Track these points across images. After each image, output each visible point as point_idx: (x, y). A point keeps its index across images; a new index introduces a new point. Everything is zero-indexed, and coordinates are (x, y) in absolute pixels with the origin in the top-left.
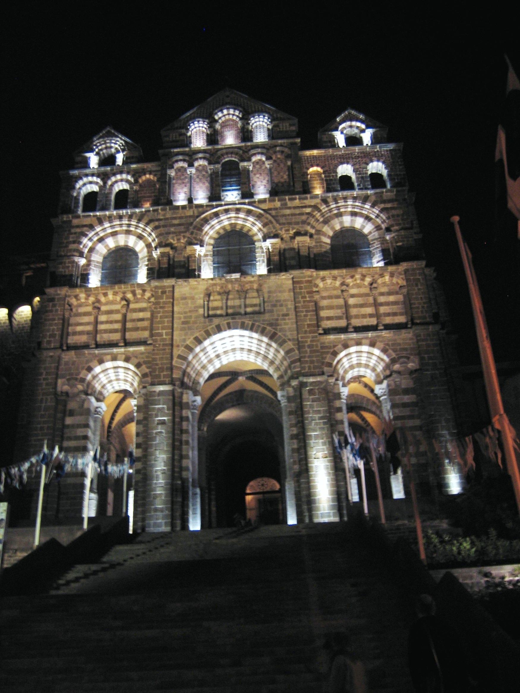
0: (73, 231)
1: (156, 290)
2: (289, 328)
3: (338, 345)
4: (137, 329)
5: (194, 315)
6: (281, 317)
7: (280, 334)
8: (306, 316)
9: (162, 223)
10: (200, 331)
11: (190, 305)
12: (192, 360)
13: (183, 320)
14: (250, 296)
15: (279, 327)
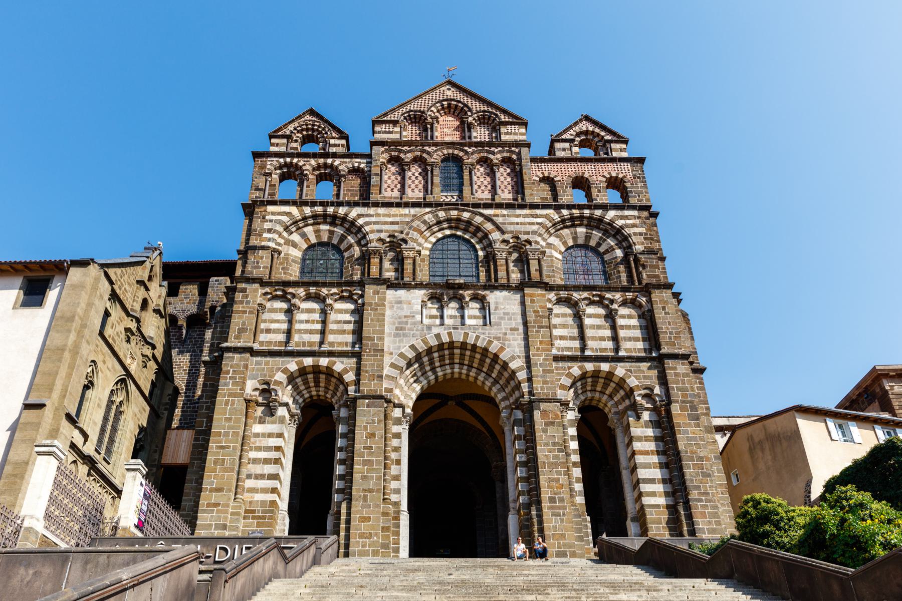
5: (410, 320)
6: (509, 332)
7: (507, 349)
8: (538, 332)
9: (373, 219)
10: (417, 339)
11: (405, 309)
13: (397, 325)
15: (506, 342)
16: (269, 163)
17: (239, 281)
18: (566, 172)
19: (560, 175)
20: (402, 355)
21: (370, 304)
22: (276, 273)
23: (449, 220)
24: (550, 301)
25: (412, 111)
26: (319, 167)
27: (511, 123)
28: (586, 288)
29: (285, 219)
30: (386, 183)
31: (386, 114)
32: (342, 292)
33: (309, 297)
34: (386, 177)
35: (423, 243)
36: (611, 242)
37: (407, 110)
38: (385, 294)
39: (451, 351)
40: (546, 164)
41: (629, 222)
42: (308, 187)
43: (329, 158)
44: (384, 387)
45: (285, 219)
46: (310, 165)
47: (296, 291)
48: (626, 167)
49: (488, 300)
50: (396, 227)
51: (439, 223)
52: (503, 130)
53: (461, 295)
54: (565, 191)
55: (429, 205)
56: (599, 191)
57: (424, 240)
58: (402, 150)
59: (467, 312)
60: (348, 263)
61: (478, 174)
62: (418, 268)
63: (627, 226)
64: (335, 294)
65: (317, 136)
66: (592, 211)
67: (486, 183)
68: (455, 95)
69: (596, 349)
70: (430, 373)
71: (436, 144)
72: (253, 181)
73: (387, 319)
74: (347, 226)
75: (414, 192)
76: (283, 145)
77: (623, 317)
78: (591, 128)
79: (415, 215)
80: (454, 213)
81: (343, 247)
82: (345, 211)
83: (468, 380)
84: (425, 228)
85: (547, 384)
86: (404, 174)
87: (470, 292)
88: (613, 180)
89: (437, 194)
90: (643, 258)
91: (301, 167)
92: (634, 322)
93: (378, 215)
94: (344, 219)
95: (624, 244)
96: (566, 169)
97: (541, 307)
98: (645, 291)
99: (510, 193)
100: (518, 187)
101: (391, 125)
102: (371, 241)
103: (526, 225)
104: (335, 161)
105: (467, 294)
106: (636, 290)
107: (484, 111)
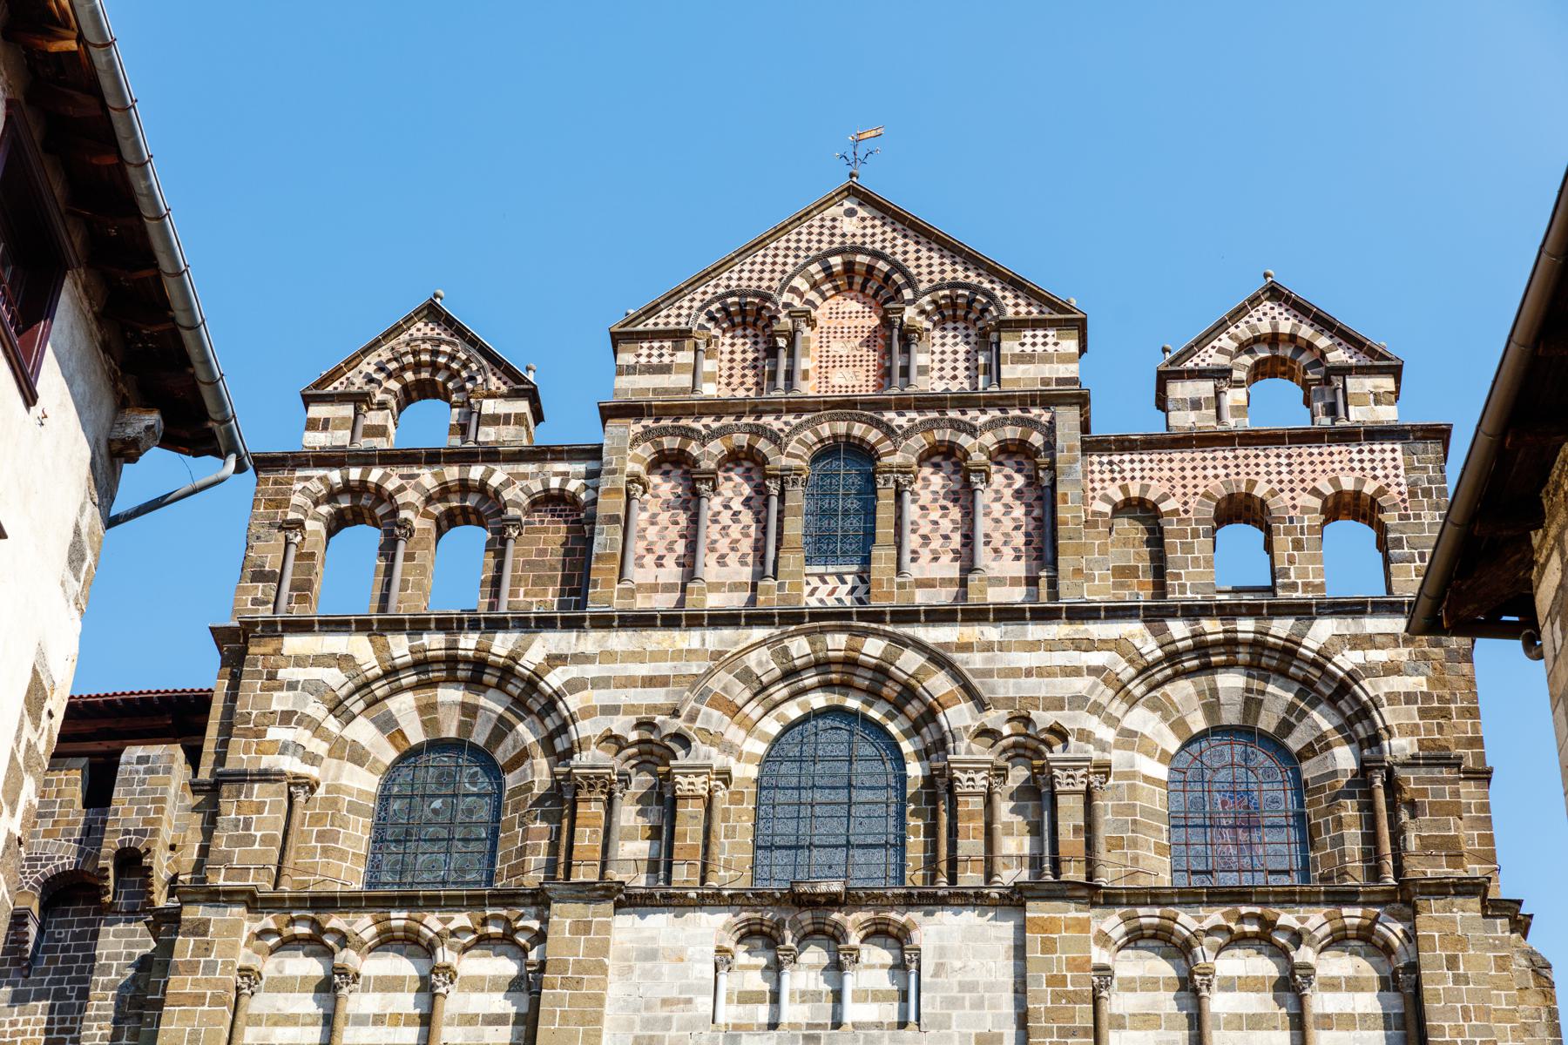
5: (678, 1015)
9: (591, 671)
13: (638, 1031)
16: (298, 486)
17: (189, 898)
18: (1199, 481)
19: (1179, 491)
21: (562, 966)
22: (298, 853)
23: (821, 665)
24: (1104, 939)
25: (732, 294)
26: (445, 491)
27: (1035, 324)
28: (1217, 896)
29: (334, 677)
30: (643, 538)
31: (652, 310)
32: (484, 922)
33: (387, 941)
34: (645, 516)
35: (738, 741)
36: (1323, 720)
37: (721, 290)
38: (608, 931)
40: (1136, 457)
42: (409, 557)
43: (476, 462)
45: (334, 677)
46: (418, 487)
47: (350, 924)
48: (1388, 455)
49: (916, 942)
50: (658, 696)
51: (790, 674)
52: (1009, 346)
53: (836, 925)
54: (1187, 548)
55: (763, 619)
56: (1298, 545)
57: (742, 733)
58: (693, 430)
59: (851, 982)
60: (515, 810)
61: (925, 497)
62: (719, 827)
63: (1370, 670)
64: (464, 929)
65: (444, 384)
66: (1264, 624)
67: (946, 526)
71: (798, 408)
72: (249, 547)
73: (608, 1010)
74: (516, 692)
75: (724, 565)
76: (341, 423)
77: (1332, 985)
78: (1285, 327)
79: (721, 653)
80: (837, 642)
81: (502, 755)
82: (510, 646)
84: (747, 694)
86: (698, 506)
87: (862, 916)
89: (791, 574)
90: (1411, 780)
91: (391, 496)
92: (1368, 1002)
93: (609, 656)
94: (507, 672)
95: (1359, 727)
96: (1199, 472)
97: (1074, 965)
98: (1402, 901)
99: (1018, 558)
100: (1042, 536)
101: (667, 344)
102: (581, 745)
103: (1055, 675)
105: (853, 922)
106: (1372, 898)
107: (955, 285)
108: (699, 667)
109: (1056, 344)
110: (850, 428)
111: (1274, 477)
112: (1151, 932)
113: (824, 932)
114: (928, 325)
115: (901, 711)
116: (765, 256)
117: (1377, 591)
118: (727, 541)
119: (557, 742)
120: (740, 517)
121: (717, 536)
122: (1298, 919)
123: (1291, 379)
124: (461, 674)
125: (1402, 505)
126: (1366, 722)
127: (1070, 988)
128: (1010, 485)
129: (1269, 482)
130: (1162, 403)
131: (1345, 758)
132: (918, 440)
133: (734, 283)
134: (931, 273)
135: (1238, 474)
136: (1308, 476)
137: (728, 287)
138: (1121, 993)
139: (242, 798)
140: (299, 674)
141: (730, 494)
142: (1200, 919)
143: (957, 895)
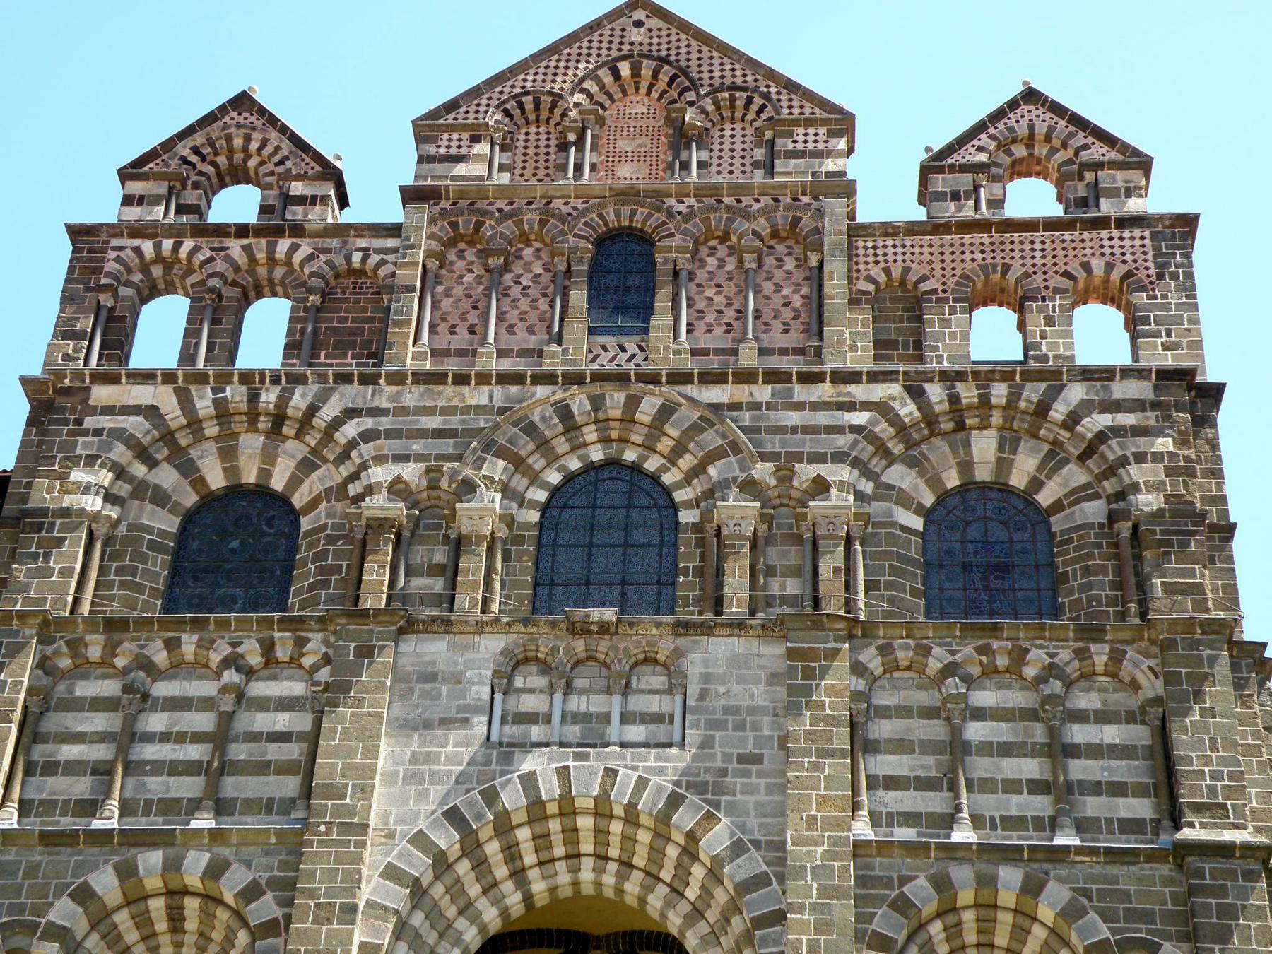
0: (90, 422)
1: (341, 643)
2: (759, 805)
3: (915, 877)
4: (262, 768)
8: (816, 767)
9: (385, 423)
10: (468, 791)
12: (431, 885)
14: (643, 686)
15: (724, 799)
19: (938, 273)
20: (420, 840)
27: (809, 123)
29: (135, 424)
31: (452, 106)
37: (517, 90)
39: (566, 820)
41: (1129, 419)
44: (358, 937)
47: (142, 647)
48: (1138, 242)
56: (1049, 321)
63: (1118, 431)
68: (655, 40)
69: (992, 819)
70: (508, 886)
74: (313, 443)
75: (514, 333)
80: (616, 399)
82: (309, 400)
83: (622, 901)
84: (531, 446)
85: (830, 933)
88: (1097, 281)
95: (1106, 484)
96: (957, 256)
99: (786, 331)
100: (810, 311)
104: (294, 248)
107: (734, 88)
108: (487, 421)
109: (826, 142)
110: (633, 213)
111: (1029, 261)
112: (906, 663)
113: (596, 660)
114: (709, 125)
115: (674, 464)
116: (558, 61)
117: (1125, 359)
118: (516, 312)
119: (350, 487)
120: (529, 291)
121: (508, 308)
122: (1049, 654)
123: (1045, 178)
124: (261, 426)
125: (1150, 287)
126: (1113, 479)
127: (828, 712)
128: (780, 267)
129: (1023, 265)
130: (925, 197)
131: (1094, 511)
132: (695, 225)
133: (528, 84)
134: (711, 78)
135: (994, 258)
136: (1060, 260)
137: (523, 87)
138: (877, 720)
139: (43, 534)
140: (106, 422)
141: (521, 271)
142: (953, 653)
143: (722, 625)
